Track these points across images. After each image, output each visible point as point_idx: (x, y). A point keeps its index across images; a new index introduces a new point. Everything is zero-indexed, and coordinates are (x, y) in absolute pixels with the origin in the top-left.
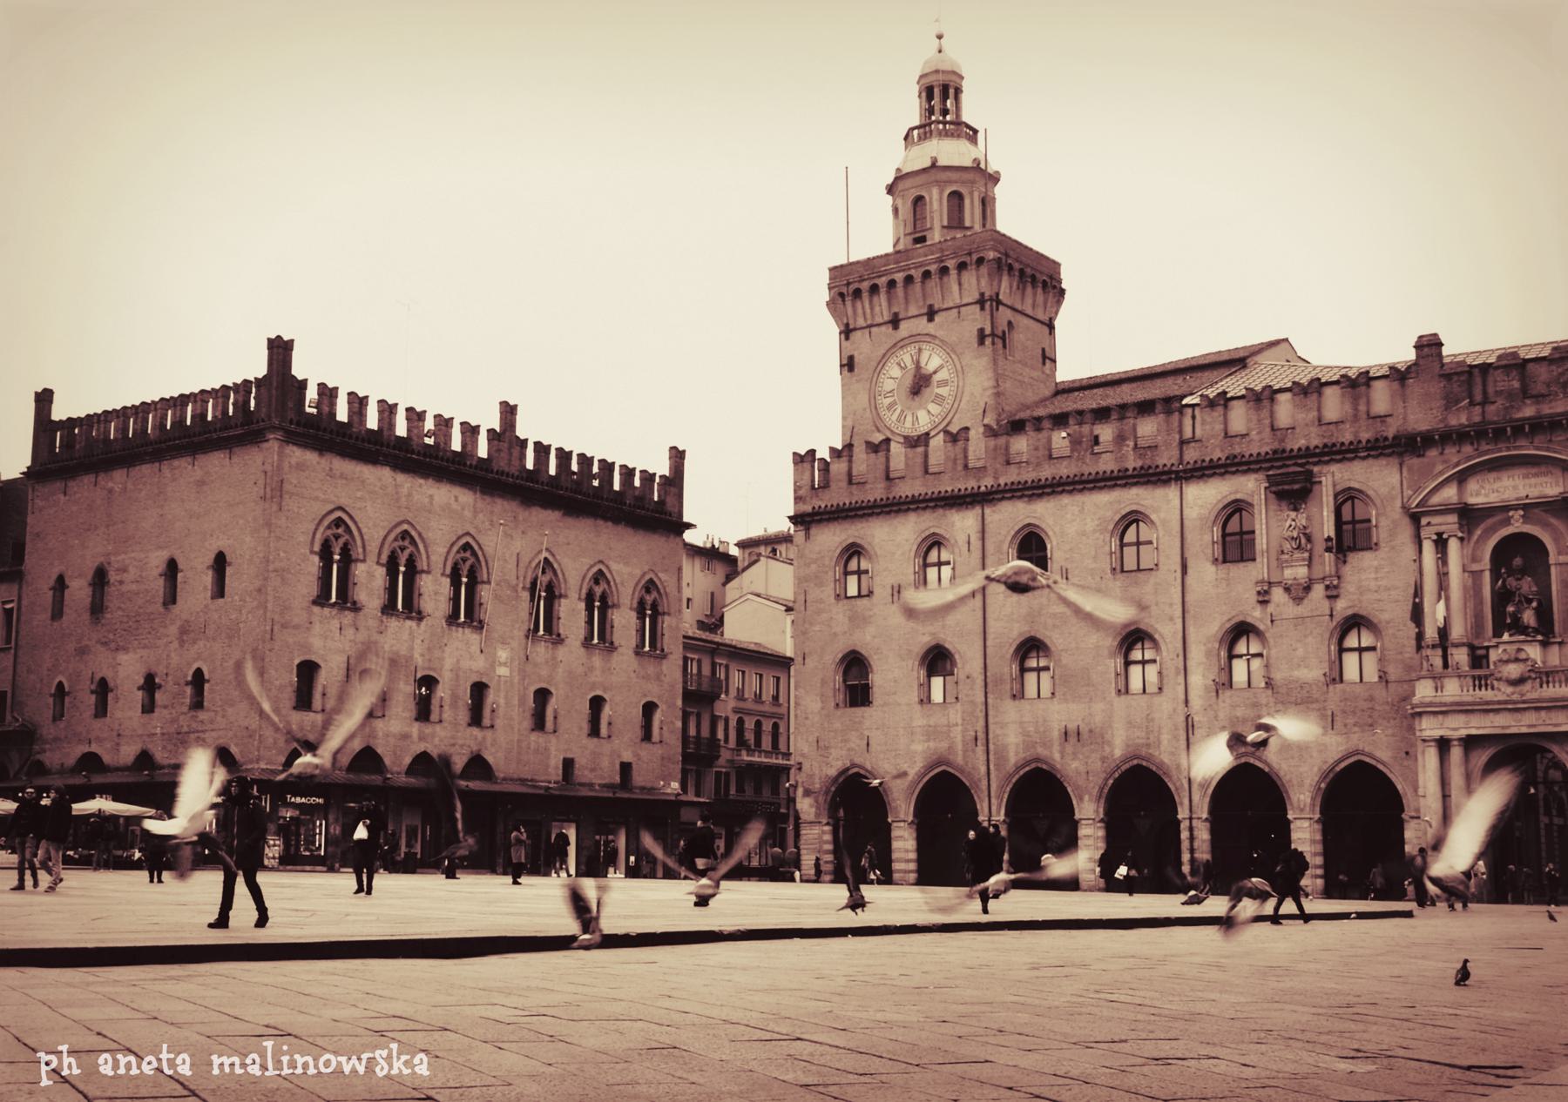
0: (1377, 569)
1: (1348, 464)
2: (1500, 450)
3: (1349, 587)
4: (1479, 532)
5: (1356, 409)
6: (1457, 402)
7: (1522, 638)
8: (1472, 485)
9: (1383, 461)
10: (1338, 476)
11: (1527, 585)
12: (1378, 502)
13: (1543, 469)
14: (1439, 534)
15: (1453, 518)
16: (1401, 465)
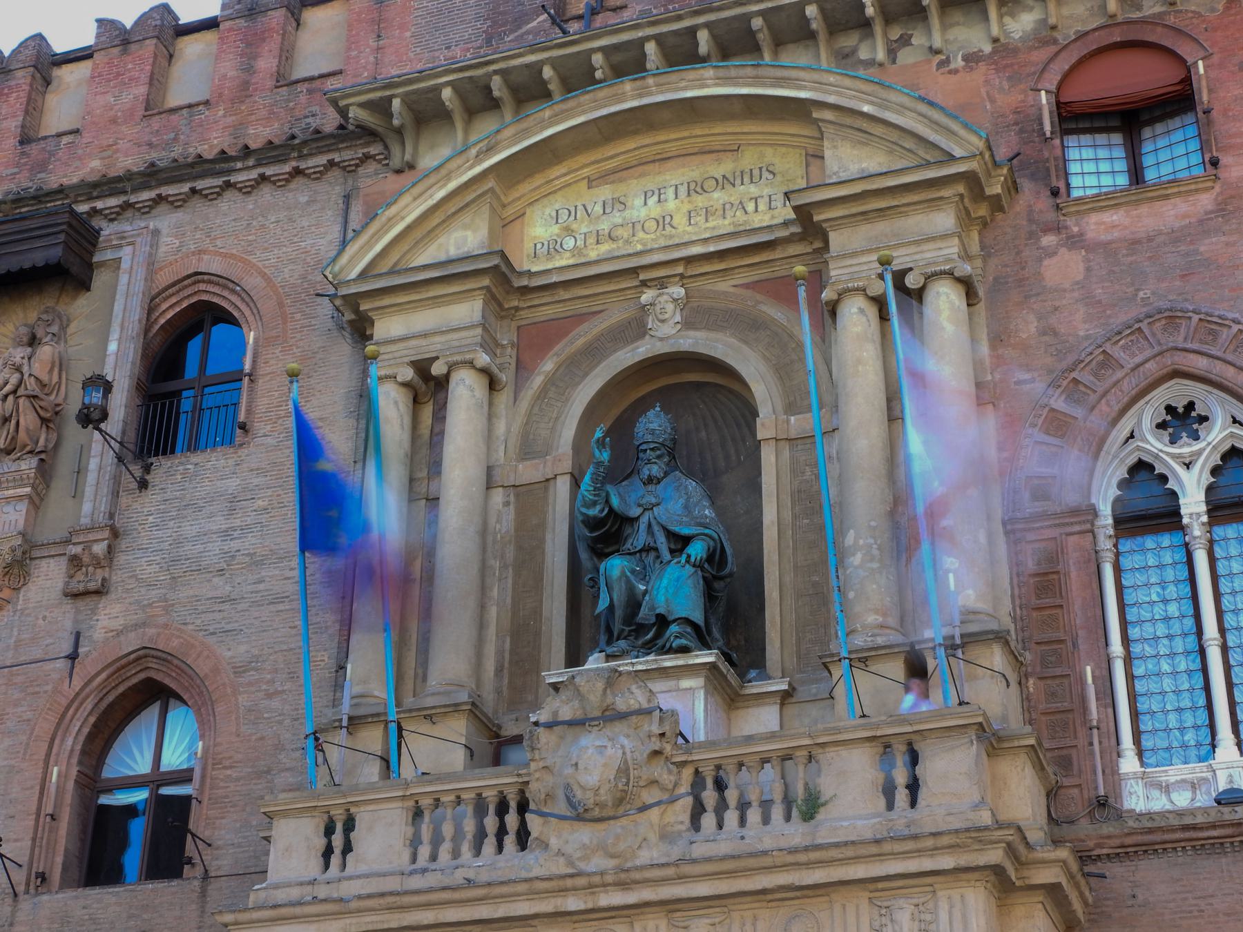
0: (233, 503)
1: (197, 203)
2: (621, 98)
3: (140, 564)
4: (548, 366)
5: (249, 70)
6: (521, 20)
7: (648, 661)
8: (540, 228)
9: (300, 192)
10: (168, 242)
11: (676, 503)
12: (267, 306)
13: (748, 159)
14: (422, 368)
15: (468, 310)
16: (347, 198)
